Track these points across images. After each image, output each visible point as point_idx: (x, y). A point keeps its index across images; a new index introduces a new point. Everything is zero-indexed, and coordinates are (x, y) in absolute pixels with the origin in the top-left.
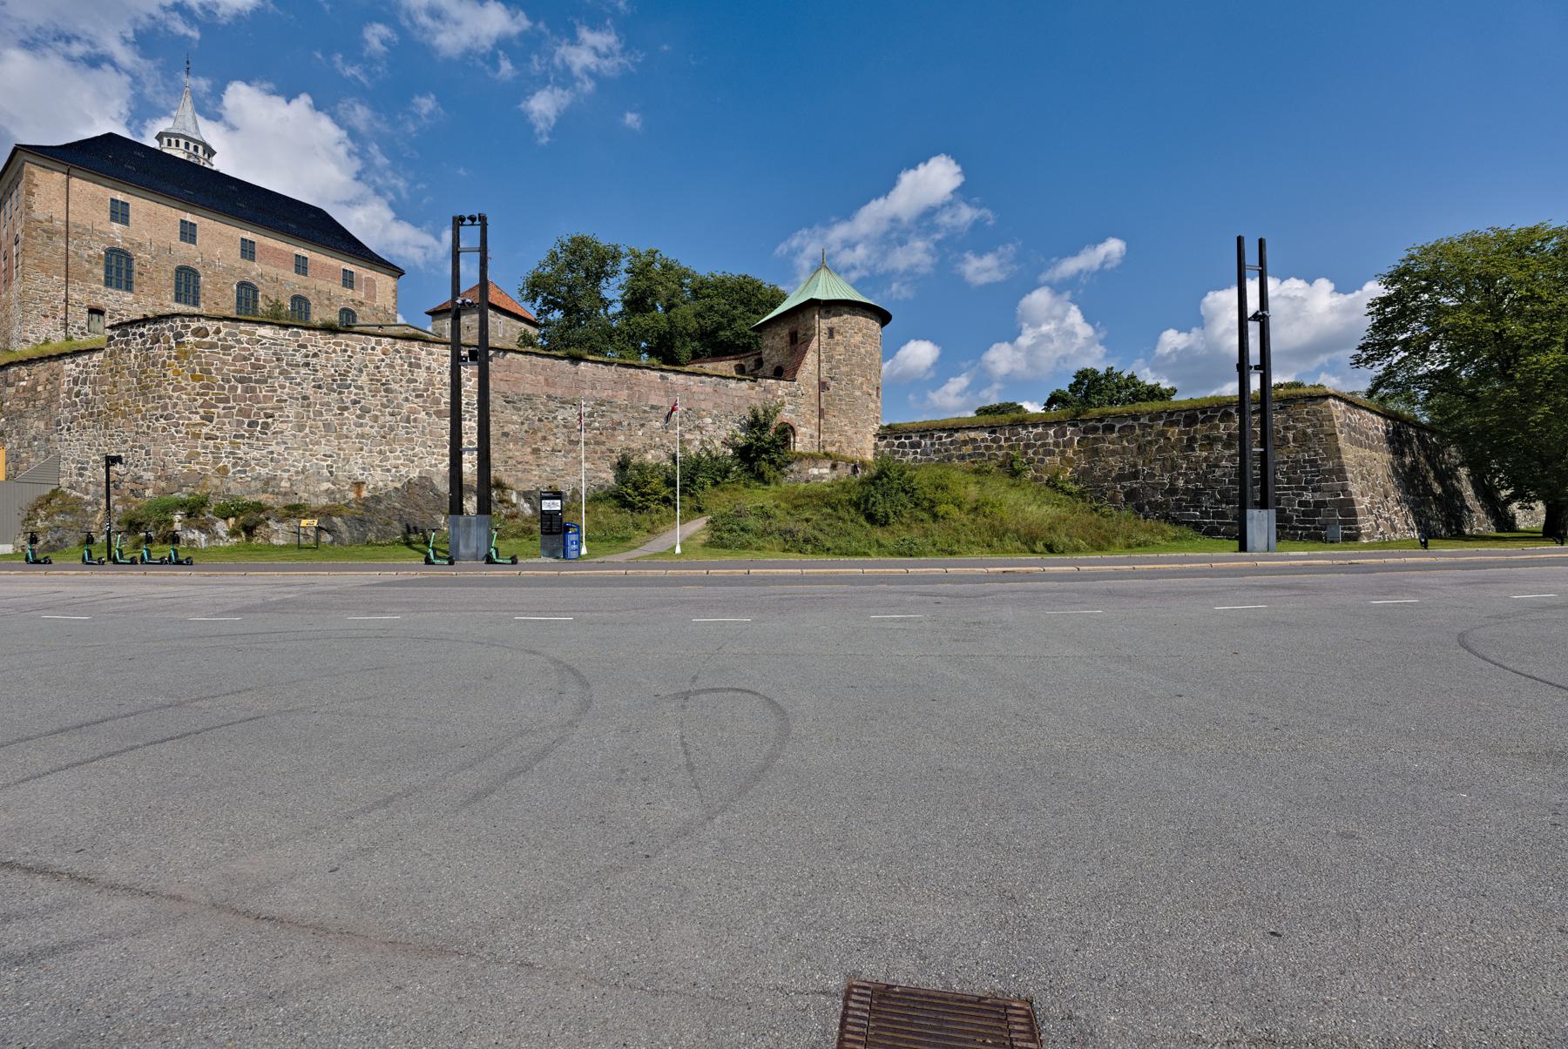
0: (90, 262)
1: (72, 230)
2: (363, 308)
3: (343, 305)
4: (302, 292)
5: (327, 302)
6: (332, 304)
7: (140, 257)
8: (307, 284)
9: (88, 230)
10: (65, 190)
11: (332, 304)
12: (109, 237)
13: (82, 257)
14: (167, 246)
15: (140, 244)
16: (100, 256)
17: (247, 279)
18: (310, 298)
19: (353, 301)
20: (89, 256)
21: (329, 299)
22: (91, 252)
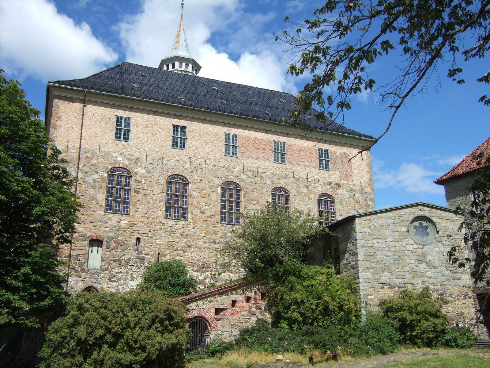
0: (94, 187)
1: (83, 156)
2: (340, 191)
3: (321, 190)
4: (281, 183)
5: (305, 190)
6: (310, 192)
7: (137, 174)
8: (286, 173)
9: (96, 153)
10: (81, 116)
11: (310, 192)
12: (112, 157)
13: (88, 183)
14: (160, 156)
15: (138, 160)
16: (103, 178)
17: (231, 178)
18: (289, 188)
19: (330, 184)
20: (95, 181)
21: (307, 187)
22: (96, 177)
